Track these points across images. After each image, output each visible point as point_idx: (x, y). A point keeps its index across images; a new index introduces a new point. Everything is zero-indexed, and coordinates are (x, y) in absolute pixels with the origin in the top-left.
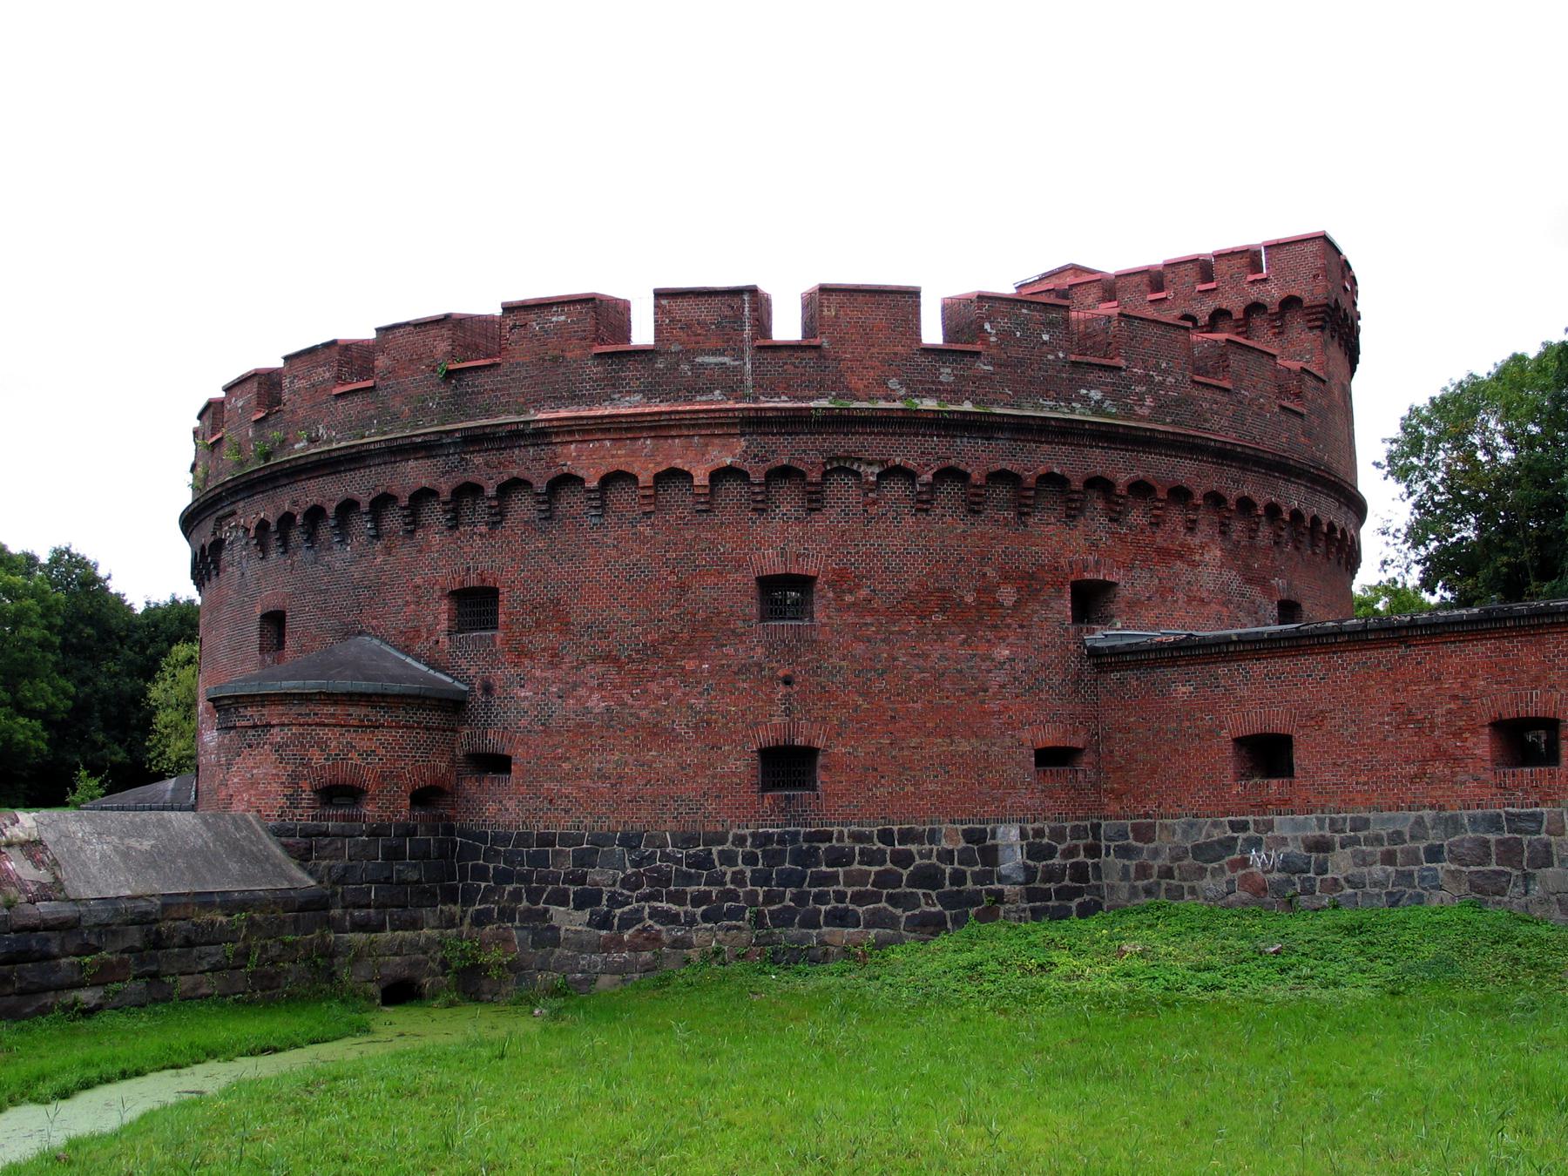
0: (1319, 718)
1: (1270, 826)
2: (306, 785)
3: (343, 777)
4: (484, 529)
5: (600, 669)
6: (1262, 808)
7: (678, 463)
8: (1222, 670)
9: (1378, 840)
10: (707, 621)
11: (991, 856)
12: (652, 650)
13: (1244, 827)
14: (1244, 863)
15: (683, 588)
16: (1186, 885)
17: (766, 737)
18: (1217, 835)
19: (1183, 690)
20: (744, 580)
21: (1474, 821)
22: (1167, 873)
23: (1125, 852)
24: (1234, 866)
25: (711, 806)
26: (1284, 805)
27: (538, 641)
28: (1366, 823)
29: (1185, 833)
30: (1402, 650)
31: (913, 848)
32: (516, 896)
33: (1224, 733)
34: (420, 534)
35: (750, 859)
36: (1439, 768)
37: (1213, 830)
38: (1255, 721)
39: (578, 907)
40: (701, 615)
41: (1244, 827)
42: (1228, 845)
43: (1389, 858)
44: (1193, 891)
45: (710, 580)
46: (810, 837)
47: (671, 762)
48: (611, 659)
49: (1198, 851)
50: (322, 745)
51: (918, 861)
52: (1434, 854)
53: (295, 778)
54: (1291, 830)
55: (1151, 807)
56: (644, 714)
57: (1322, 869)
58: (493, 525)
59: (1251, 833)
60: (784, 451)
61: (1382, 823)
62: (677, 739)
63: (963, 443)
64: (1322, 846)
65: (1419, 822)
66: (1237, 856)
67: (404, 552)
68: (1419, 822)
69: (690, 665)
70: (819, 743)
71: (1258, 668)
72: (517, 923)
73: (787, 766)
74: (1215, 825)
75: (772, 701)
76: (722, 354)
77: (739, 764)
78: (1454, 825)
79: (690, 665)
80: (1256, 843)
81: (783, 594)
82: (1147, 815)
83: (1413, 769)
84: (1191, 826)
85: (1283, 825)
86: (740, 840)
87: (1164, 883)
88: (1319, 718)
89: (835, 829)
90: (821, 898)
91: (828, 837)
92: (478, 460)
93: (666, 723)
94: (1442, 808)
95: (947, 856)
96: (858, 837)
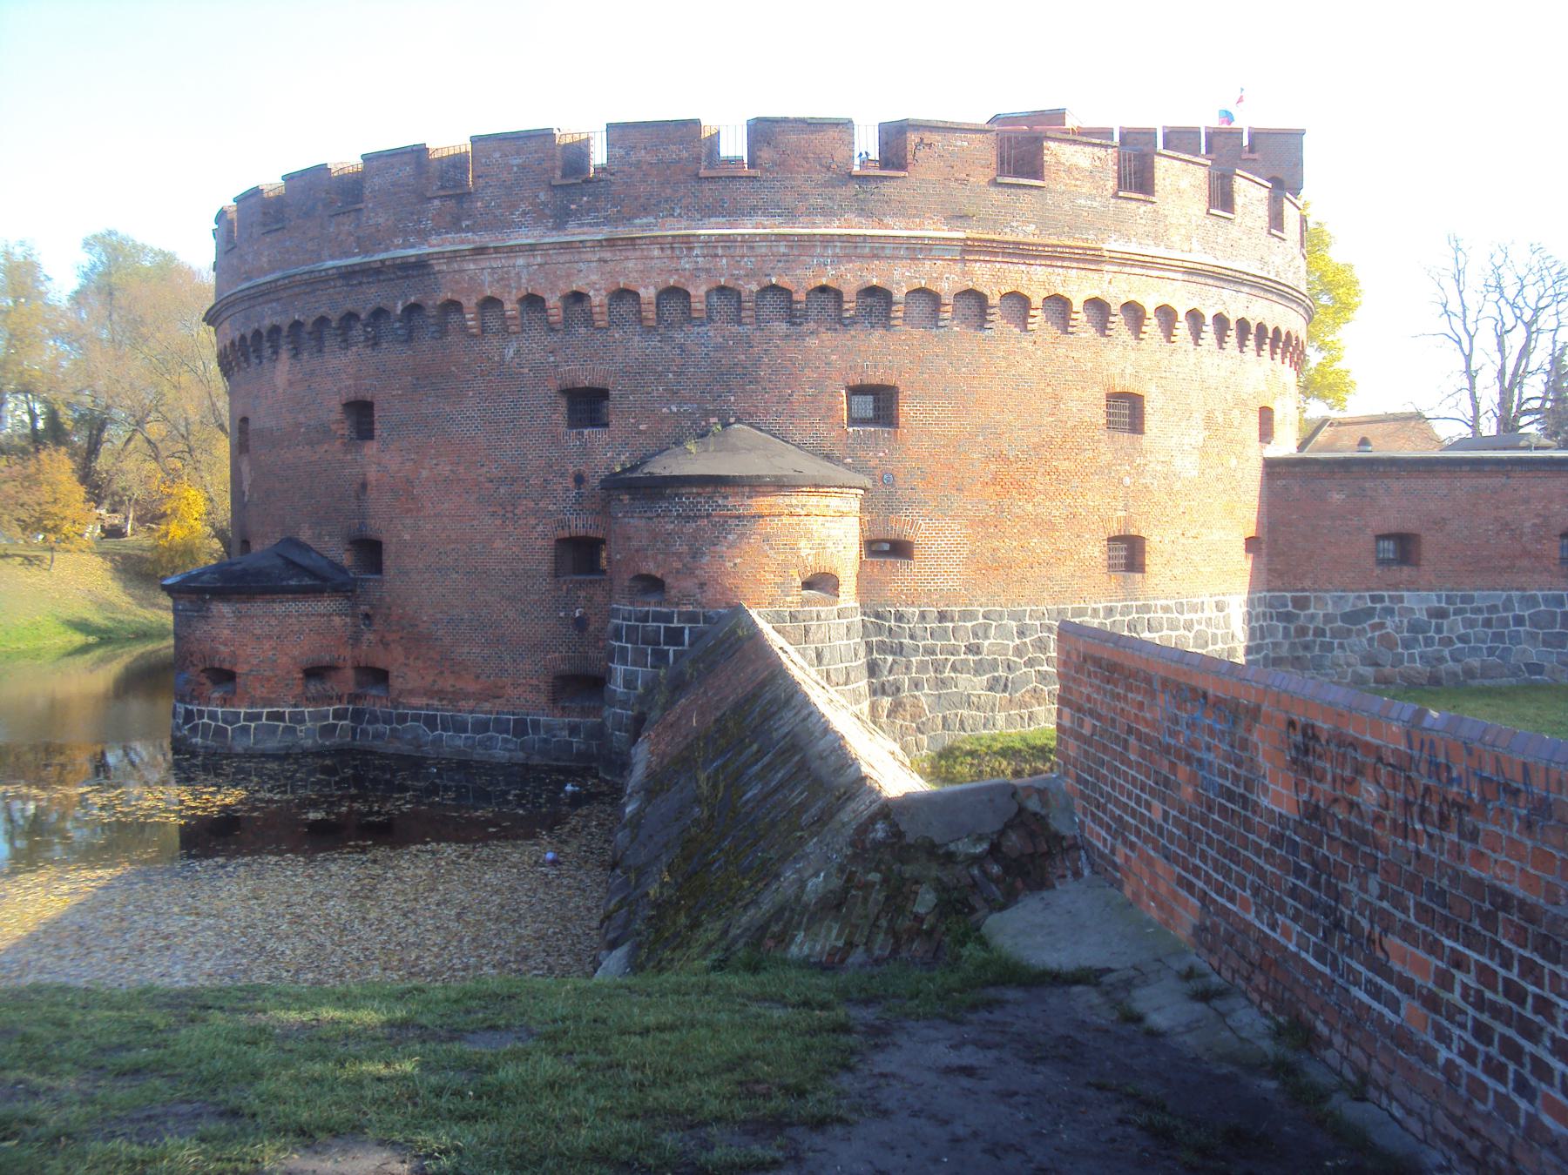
1: (1401, 599)
2: (794, 572)
3: (825, 565)
6: (1396, 587)
7: (1060, 291)
9: (1479, 610)
11: (1227, 619)
13: (1381, 599)
14: (1382, 626)
16: (1336, 642)
17: (1114, 530)
18: (1361, 605)
19: (1337, 497)
20: (1099, 395)
21: (1546, 599)
22: (1320, 632)
23: (1288, 617)
24: (1374, 627)
26: (1412, 586)
28: (1471, 599)
29: (1335, 604)
30: (1504, 480)
31: (1195, 617)
32: (923, 667)
33: (1369, 531)
36: (1525, 563)
37: (1351, 602)
38: (1393, 526)
39: (977, 672)
41: (1381, 599)
42: (1370, 613)
43: (1487, 623)
44: (1341, 646)
49: (1346, 617)
50: (809, 535)
51: (1196, 627)
52: (1519, 621)
54: (1417, 603)
55: (1308, 583)
57: (1439, 630)
59: (1387, 603)
61: (1482, 598)
62: (1052, 526)
63: (1227, 293)
64: (1441, 614)
65: (1509, 598)
66: (1376, 620)
68: (1509, 598)
71: (1397, 485)
72: (926, 691)
74: (1359, 598)
77: (1096, 551)
78: (1531, 601)
80: (1389, 612)
82: (1303, 590)
83: (1505, 563)
84: (1341, 598)
85: (1410, 599)
87: (1319, 640)
89: (1152, 602)
91: (1146, 609)
94: (1524, 589)
95: (1209, 622)
96: (1166, 609)
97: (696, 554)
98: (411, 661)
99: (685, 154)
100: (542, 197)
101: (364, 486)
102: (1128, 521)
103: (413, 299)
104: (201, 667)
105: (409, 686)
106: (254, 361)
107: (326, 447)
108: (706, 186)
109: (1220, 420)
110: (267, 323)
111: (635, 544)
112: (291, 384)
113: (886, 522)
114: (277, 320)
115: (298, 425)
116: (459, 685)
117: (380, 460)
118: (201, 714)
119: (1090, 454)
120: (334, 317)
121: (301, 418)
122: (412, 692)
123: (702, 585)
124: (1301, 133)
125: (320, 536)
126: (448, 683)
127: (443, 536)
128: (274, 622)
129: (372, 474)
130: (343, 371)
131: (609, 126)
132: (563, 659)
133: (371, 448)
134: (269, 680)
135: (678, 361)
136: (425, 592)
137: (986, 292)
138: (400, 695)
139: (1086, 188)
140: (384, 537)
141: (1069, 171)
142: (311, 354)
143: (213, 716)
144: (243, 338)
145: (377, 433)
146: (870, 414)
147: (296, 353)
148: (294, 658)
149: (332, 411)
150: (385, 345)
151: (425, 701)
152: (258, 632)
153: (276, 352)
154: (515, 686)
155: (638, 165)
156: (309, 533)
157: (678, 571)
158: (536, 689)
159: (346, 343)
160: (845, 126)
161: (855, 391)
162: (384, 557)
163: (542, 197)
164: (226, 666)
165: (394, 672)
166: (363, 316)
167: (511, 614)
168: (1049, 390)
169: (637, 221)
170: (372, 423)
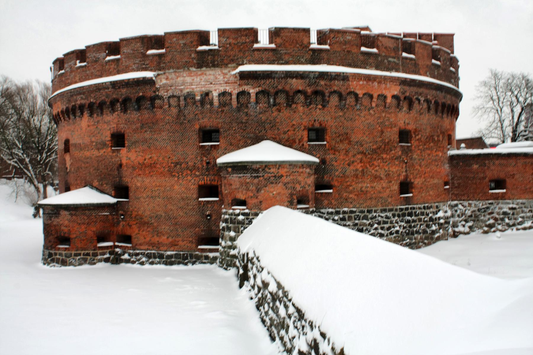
0: (513, 176)
2: (295, 197)
4: (320, 107)
5: (359, 156)
8: (487, 162)
10: (388, 142)
12: (374, 151)
15: (382, 132)
19: (475, 167)
20: (396, 130)
25: (390, 200)
27: (341, 146)
34: (294, 106)
35: (399, 216)
40: (387, 141)
45: (389, 130)
46: (411, 208)
47: (380, 186)
48: (363, 153)
53: (291, 195)
56: (373, 171)
58: (324, 106)
60: (410, 91)
62: (381, 179)
67: (286, 113)
69: (384, 156)
70: (412, 181)
71: (497, 162)
73: (405, 187)
75: (402, 168)
76: (395, 58)
79: (384, 156)
81: (404, 135)
86: (396, 210)
88: (513, 176)
90: (414, 227)
91: (414, 208)
92: (322, 83)
93: (378, 174)
96: (420, 208)
97: (258, 190)
98: (141, 232)
99: (248, 40)
100: (193, 56)
101: (121, 165)
102: (407, 177)
103: (141, 94)
104: (56, 236)
105: (140, 242)
106: (72, 117)
107: (104, 150)
108: (256, 53)
109: (436, 139)
110: (79, 102)
111: (233, 187)
112: (89, 126)
113: (323, 177)
114: (83, 102)
115: (92, 142)
116: (161, 240)
117: (127, 156)
118: (56, 254)
119: (393, 152)
120: (108, 101)
121: (93, 139)
122: (141, 245)
123: (261, 202)
124: (452, 36)
125: (102, 185)
126: (156, 239)
127: (154, 184)
128: (86, 218)
129: (124, 162)
130: (111, 122)
131: (219, 30)
132: (202, 231)
133: (124, 151)
134: (84, 240)
135: (246, 118)
136: (146, 206)
137: (358, 92)
138: (136, 245)
139: (393, 54)
140: (130, 185)
141: (386, 48)
142: (98, 115)
143: (61, 254)
144: (67, 109)
145: (126, 145)
146: (315, 138)
147: (91, 115)
148: (94, 231)
149: (107, 137)
150: (129, 112)
151: (146, 247)
152: (79, 222)
153: (82, 114)
154: (183, 241)
155: (230, 44)
156: (97, 183)
157: (251, 197)
158: (191, 242)
159: (113, 111)
160: (307, 31)
161: (309, 130)
162: (130, 192)
163: (193, 56)
164: (66, 235)
165: (133, 235)
166: (120, 100)
167: (181, 214)
168: (380, 128)
169: (230, 65)
170: (124, 141)
